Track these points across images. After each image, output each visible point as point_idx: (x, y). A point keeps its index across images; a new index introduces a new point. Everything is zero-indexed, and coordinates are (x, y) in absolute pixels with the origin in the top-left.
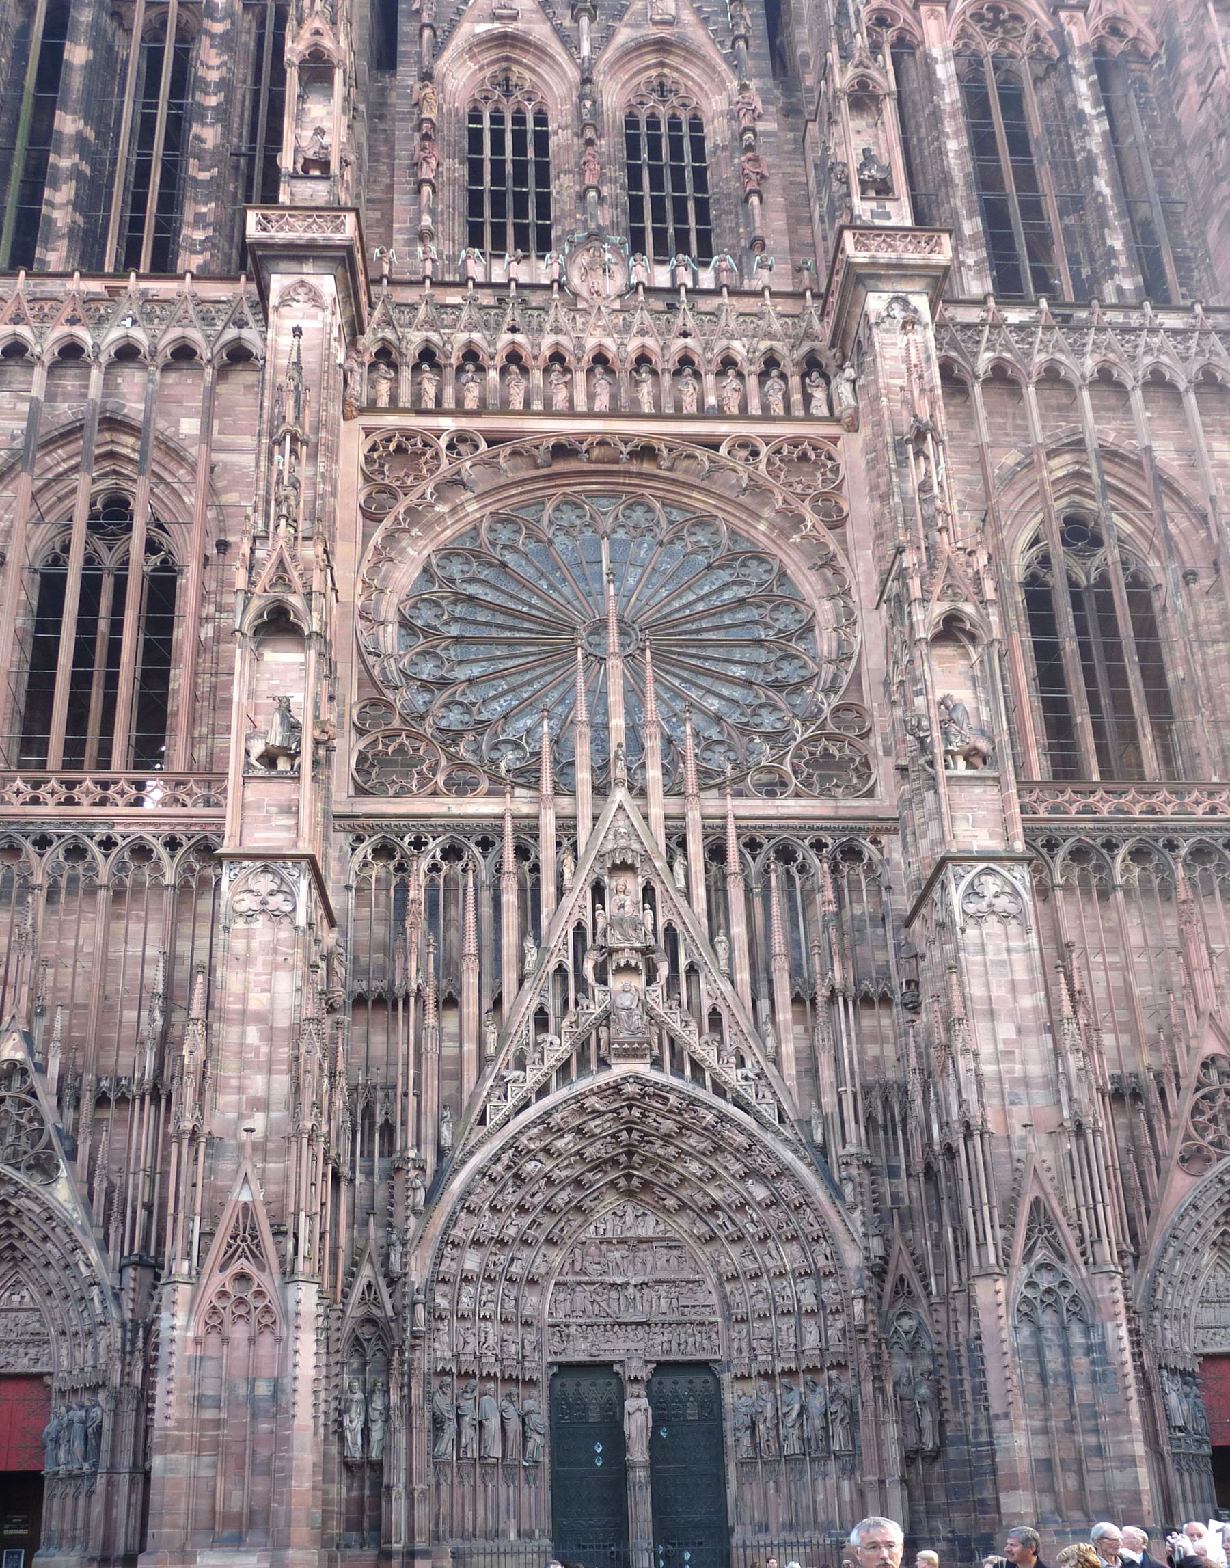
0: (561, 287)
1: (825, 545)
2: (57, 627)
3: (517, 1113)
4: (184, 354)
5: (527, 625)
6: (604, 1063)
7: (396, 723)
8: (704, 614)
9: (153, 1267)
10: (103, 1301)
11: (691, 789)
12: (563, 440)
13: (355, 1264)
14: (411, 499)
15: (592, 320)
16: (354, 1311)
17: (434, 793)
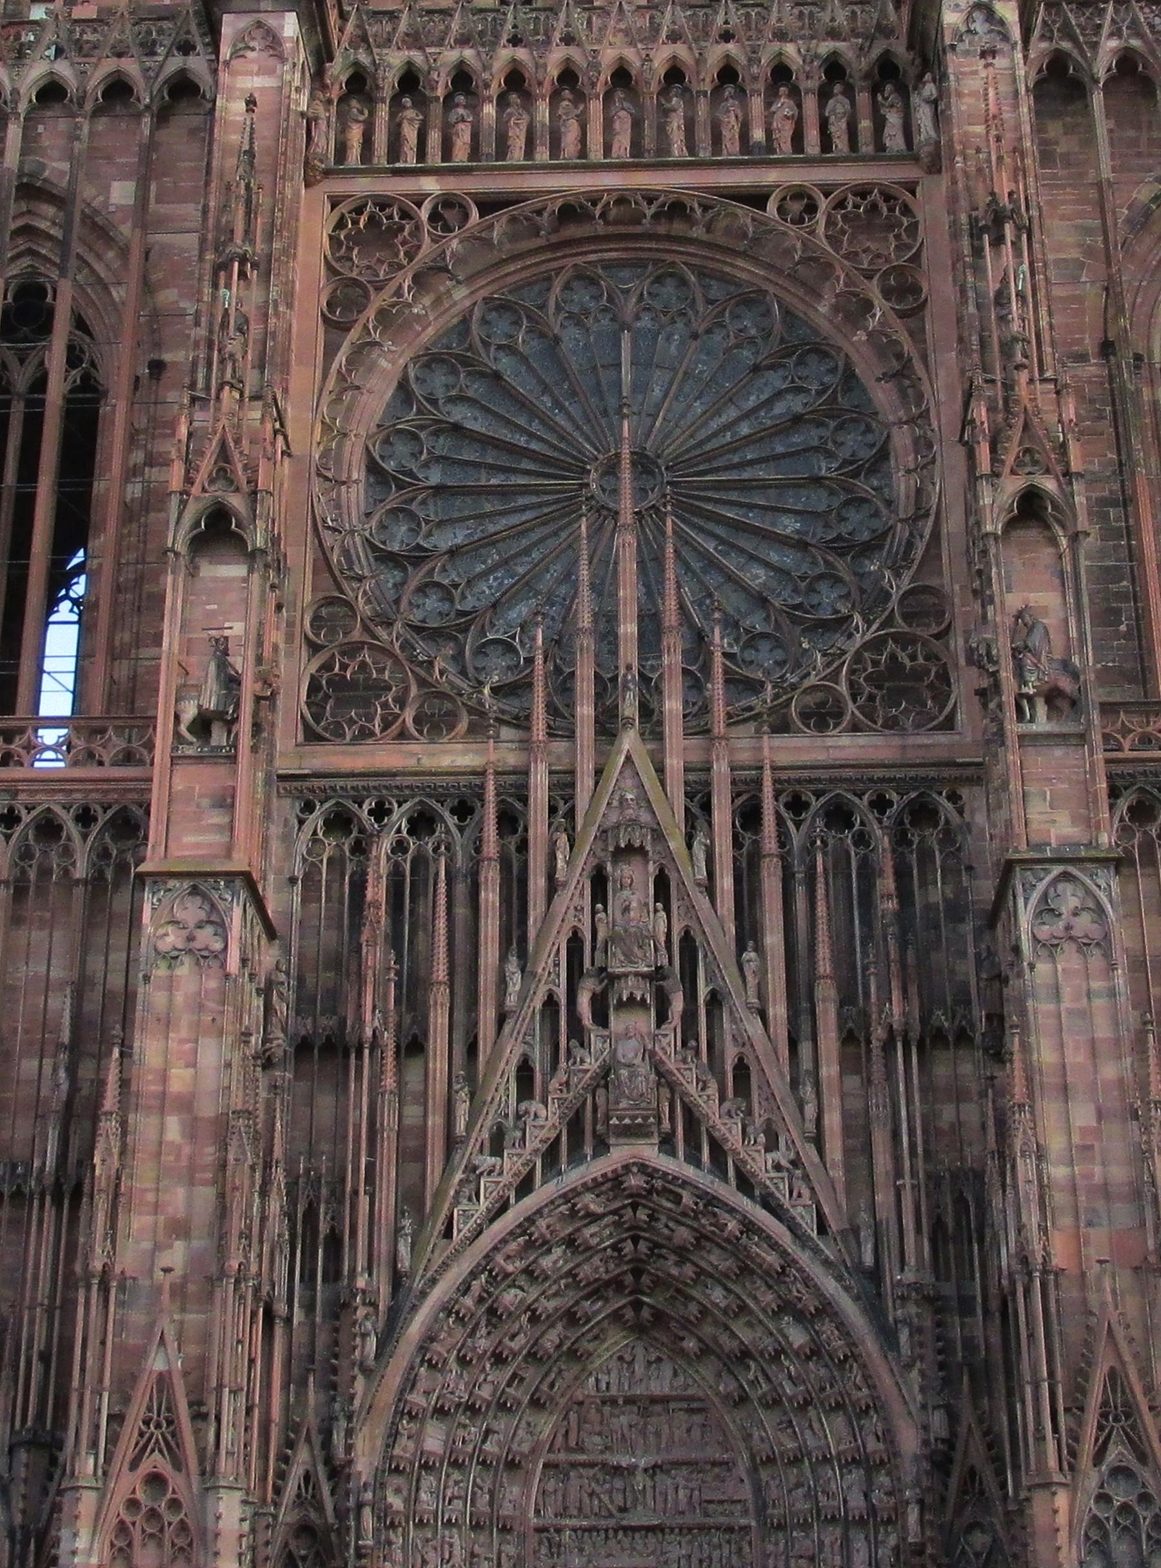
3: (492, 1220)
5: (526, 465)
8: (748, 440)
11: (719, 728)
13: (290, 1444)
16: (287, 1515)
17: (403, 735)
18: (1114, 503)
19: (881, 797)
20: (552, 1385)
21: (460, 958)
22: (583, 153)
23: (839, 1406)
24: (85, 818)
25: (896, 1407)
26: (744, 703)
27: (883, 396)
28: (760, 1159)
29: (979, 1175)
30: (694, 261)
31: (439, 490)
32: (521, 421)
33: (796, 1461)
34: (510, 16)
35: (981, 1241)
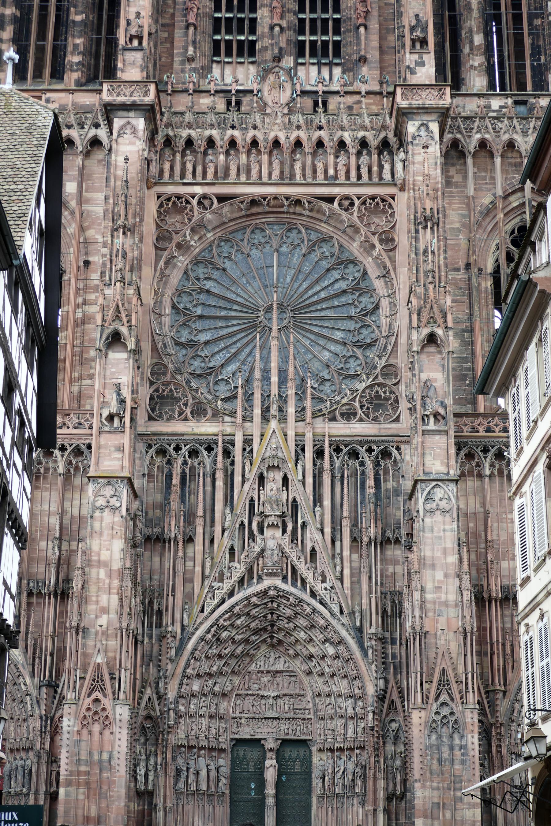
5: (235, 307)
6: (260, 579)
9: (54, 687)
10: (31, 704)
12: (255, 198)
13: (143, 687)
16: (142, 713)
17: (186, 419)
19: (370, 448)
21: (208, 507)
22: (260, 177)
23: (346, 676)
25: (367, 678)
26: (318, 408)
29: (400, 593)
31: (201, 317)
32: (233, 289)
34: (231, 116)
35: (400, 617)
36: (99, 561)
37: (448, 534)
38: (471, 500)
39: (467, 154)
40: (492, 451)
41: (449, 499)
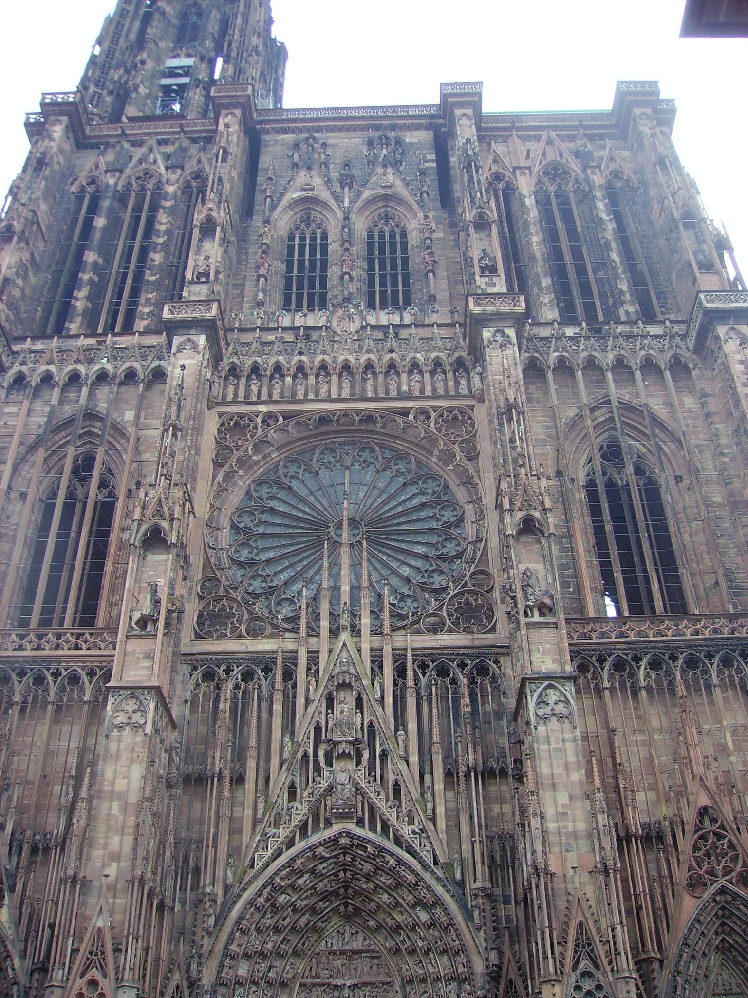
0: (327, 329)
1: (467, 471)
2: (47, 536)
3: (274, 860)
4: (130, 376)
5: (301, 525)
6: (328, 823)
7: (221, 591)
11: (387, 630)
13: (170, 971)
14: (241, 453)
15: (342, 346)
17: (240, 637)
18: (564, 537)
19: (463, 662)
20: (304, 944)
21: (263, 737)
22: (329, 395)
23: (445, 951)
24: (91, 674)
25: (472, 950)
27: (461, 494)
28: (405, 828)
29: (512, 837)
30: (378, 441)
31: (263, 535)
32: (301, 507)
33: (424, 980)
36: (112, 792)
37: (569, 745)
38: (590, 720)
39: (546, 369)
40: (610, 660)
41: (567, 701)
